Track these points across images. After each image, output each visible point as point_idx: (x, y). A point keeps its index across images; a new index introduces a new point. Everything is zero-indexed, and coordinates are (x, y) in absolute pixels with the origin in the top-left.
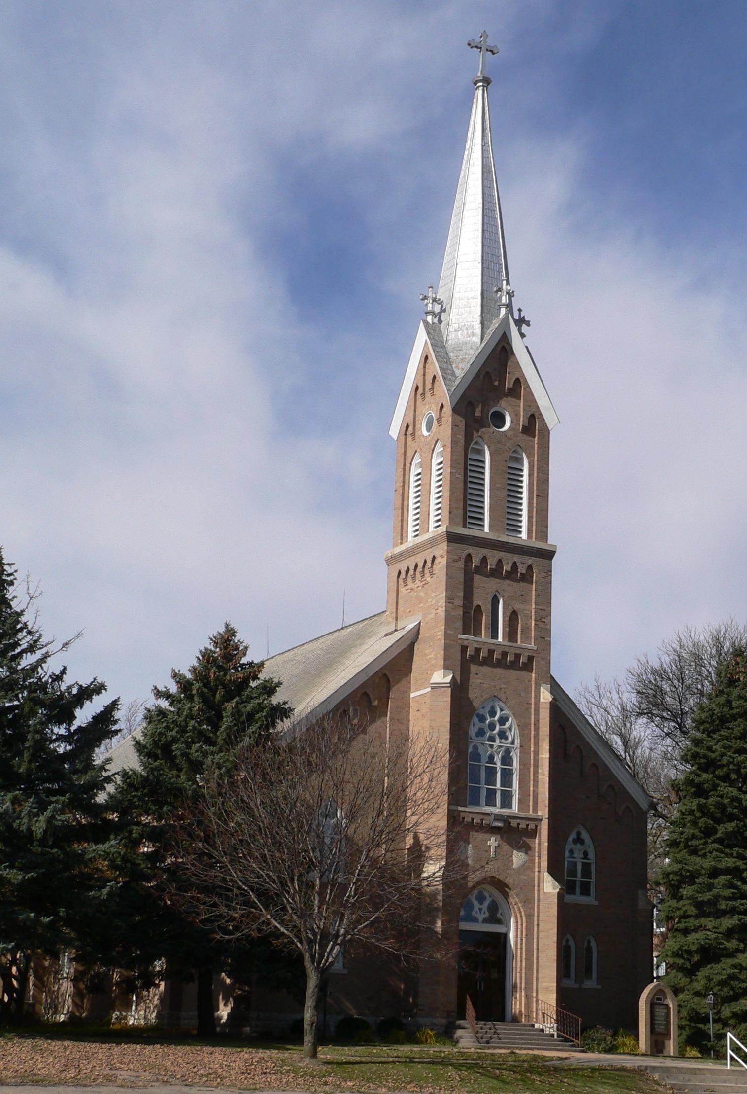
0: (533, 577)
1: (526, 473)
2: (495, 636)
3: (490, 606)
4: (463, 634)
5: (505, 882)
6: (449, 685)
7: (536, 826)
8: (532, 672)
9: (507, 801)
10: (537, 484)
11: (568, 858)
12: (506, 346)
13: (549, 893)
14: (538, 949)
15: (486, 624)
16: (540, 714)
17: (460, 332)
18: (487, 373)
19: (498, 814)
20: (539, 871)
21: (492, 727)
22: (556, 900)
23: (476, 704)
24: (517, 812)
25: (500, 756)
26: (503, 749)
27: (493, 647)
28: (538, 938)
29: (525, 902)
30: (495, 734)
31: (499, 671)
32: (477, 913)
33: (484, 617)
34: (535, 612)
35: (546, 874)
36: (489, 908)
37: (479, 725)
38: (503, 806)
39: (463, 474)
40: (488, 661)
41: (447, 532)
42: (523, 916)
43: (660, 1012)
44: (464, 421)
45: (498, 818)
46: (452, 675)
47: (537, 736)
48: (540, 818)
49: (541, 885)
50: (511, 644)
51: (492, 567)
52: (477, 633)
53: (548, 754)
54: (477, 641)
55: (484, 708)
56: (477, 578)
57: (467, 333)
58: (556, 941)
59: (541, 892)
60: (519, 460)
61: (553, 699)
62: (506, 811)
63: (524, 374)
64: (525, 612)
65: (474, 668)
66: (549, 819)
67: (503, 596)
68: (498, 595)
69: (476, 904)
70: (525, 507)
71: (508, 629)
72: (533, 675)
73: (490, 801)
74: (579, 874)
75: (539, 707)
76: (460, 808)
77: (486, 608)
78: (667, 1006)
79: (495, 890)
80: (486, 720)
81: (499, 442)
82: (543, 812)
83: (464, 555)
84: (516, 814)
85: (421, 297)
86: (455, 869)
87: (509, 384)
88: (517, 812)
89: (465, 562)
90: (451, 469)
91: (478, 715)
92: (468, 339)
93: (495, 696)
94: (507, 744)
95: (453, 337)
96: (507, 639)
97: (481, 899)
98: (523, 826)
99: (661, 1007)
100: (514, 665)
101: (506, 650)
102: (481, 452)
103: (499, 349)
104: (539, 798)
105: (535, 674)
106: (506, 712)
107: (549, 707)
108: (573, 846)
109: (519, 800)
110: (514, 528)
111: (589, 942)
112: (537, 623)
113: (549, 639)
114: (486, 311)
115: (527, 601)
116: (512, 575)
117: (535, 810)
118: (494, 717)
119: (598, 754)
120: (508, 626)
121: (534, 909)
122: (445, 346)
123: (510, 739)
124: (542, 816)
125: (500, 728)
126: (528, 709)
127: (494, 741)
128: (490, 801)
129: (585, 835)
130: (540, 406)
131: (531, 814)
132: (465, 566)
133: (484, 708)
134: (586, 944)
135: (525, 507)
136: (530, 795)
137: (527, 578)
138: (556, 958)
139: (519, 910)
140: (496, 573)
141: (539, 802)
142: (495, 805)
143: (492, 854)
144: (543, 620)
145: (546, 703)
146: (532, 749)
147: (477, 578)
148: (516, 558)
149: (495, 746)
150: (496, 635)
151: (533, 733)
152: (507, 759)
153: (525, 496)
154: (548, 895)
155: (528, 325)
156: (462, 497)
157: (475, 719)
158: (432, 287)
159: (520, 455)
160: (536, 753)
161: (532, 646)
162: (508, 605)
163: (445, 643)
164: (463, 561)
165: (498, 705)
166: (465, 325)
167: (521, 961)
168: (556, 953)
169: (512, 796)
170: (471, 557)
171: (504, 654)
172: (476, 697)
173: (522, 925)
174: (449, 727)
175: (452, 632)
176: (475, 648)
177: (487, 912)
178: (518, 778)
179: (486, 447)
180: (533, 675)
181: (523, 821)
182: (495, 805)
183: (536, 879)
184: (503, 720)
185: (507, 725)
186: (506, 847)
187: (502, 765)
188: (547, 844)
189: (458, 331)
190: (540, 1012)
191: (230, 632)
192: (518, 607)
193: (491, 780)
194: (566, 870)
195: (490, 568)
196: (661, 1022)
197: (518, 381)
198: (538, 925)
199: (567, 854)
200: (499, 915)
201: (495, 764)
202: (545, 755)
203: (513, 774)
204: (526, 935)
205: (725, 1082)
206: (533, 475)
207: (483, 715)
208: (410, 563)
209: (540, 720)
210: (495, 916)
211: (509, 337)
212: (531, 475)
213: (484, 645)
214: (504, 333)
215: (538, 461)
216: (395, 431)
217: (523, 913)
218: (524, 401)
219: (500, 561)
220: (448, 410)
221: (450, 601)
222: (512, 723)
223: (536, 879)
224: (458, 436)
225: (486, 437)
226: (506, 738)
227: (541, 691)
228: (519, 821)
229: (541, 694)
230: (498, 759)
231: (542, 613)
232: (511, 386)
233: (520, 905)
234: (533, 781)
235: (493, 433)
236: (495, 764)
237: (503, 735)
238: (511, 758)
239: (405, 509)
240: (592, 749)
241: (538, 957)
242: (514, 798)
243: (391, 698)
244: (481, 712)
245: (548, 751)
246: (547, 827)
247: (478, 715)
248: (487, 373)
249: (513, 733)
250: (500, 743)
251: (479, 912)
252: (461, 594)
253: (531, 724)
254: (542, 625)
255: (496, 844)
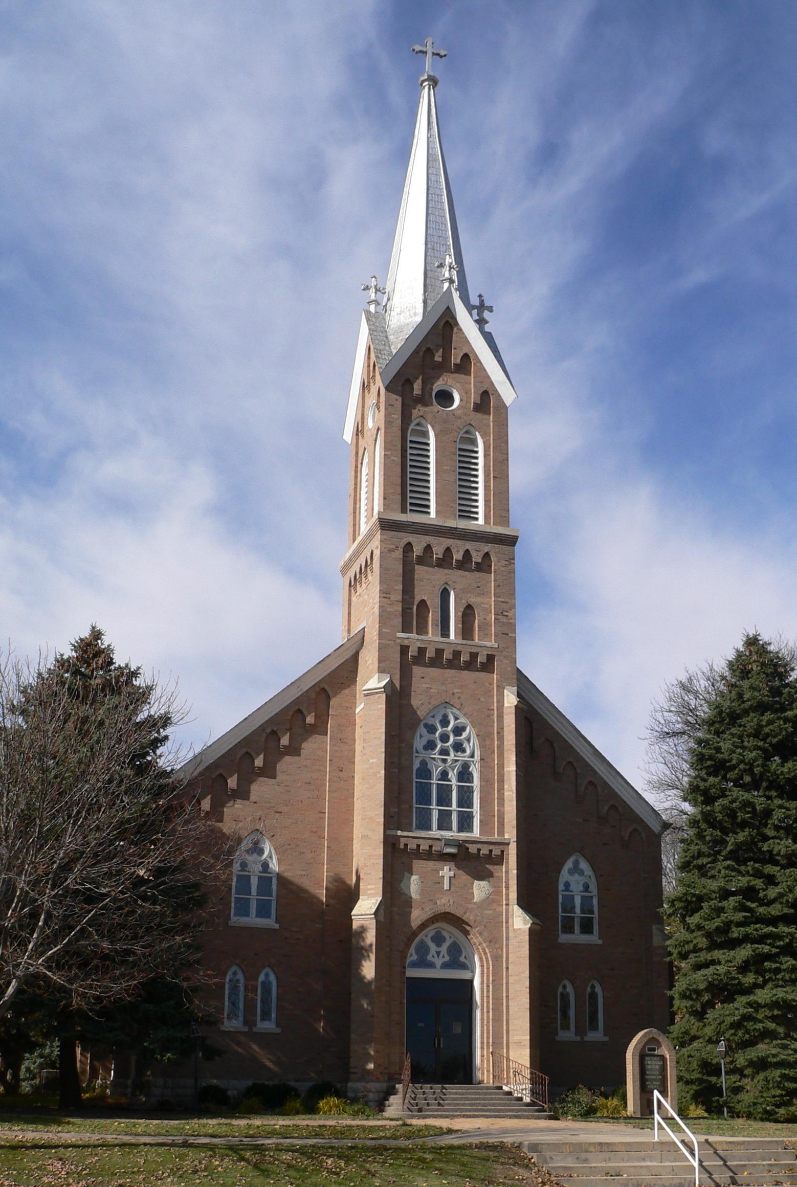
0: (491, 566)
1: (481, 455)
2: (445, 632)
3: (438, 601)
4: (403, 632)
5: (464, 918)
6: (383, 690)
7: (502, 852)
8: (493, 673)
9: (465, 822)
10: (493, 464)
11: (562, 891)
12: (451, 321)
13: (520, 929)
14: (507, 997)
15: (432, 620)
16: (505, 721)
17: (402, 315)
18: (428, 349)
19: (451, 838)
20: (507, 905)
21: (444, 738)
22: (527, 938)
23: (421, 713)
24: (478, 836)
25: (455, 771)
26: (459, 764)
27: (441, 646)
28: (507, 983)
29: (490, 941)
30: (448, 747)
31: (450, 673)
32: (433, 956)
33: (430, 613)
34: (495, 605)
35: (516, 907)
36: (449, 951)
37: (427, 737)
38: (461, 829)
39: (400, 456)
40: (437, 661)
41: (379, 518)
42: (489, 958)
43: (653, 1065)
44: (400, 399)
45: (449, 843)
46: (389, 679)
47: (501, 747)
48: (506, 842)
49: (510, 920)
50: (464, 642)
51: (438, 556)
52: (422, 630)
53: (515, 766)
54: (421, 640)
55: (433, 717)
56: (420, 570)
57: (410, 315)
58: (528, 986)
59: (510, 929)
60: (474, 442)
61: (519, 702)
62: (463, 835)
63: (473, 349)
64: (482, 605)
65: (417, 671)
66: (517, 842)
67: (454, 589)
68: (447, 587)
69: (433, 947)
70: (481, 492)
71: (461, 626)
72: (495, 677)
73: (444, 824)
74: (578, 910)
75: (503, 712)
76: (399, 833)
77: (434, 604)
78: (663, 1058)
79: (454, 928)
80: (436, 730)
81: (445, 422)
82: (511, 834)
83: (402, 544)
84: (478, 838)
85: (362, 287)
86: (173, 853)
87: (456, 359)
88: (478, 836)
89: (404, 552)
90: (385, 451)
91: (426, 726)
92: (410, 320)
93: (446, 702)
94: (464, 757)
95: (396, 321)
96: (461, 637)
97: (438, 939)
98: (485, 851)
99: (655, 1058)
100: (471, 665)
101: (459, 648)
102: (425, 434)
103: (442, 323)
104: (505, 819)
105: (497, 675)
106: (462, 720)
107: (514, 711)
108: (570, 877)
109: (481, 821)
110: (467, 513)
111: (593, 987)
112: (498, 617)
113: (513, 635)
114: (430, 290)
115: (486, 594)
116: (465, 563)
117: (501, 832)
118: (447, 727)
119: (596, 771)
120: (461, 622)
121: (502, 949)
122: (386, 332)
123: (468, 752)
124: (510, 839)
125: (454, 740)
126: (490, 716)
127: (448, 755)
128: (444, 824)
129: (584, 865)
130: (493, 381)
131: (496, 837)
132: (404, 556)
133: (433, 717)
134: (589, 990)
135: (481, 492)
136: (494, 816)
137: (484, 566)
138: (528, 1006)
139: (484, 951)
140: (445, 561)
141: (505, 824)
142: (450, 829)
143: (446, 887)
144: (506, 614)
145: (510, 707)
146: (496, 762)
147: (420, 570)
148: (469, 545)
149: (449, 760)
150: (447, 633)
151: (496, 743)
152: (465, 775)
153: (481, 479)
154: (518, 932)
155: (491, 311)
156: (399, 481)
157: (422, 730)
158: (375, 277)
159: (473, 435)
160: (501, 766)
161: (492, 643)
162: (461, 599)
163: (379, 643)
164: (402, 550)
165: (452, 712)
166: (407, 307)
167: (488, 1012)
168: (528, 1000)
169: (473, 817)
170: (412, 546)
171: (457, 654)
172: (422, 704)
173: (488, 968)
174: (384, 738)
175: (389, 631)
176: (419, 648)
177: (446, 955)
178: (479, 796)
179: (430, 427)
180: (495, 677)
181: (485, 845)
182: (450, 829)
183: (504, 914)
184: (458, 731)
185: (464, 735)
186: (464, 877)
187: (459, 781)
188: (515, 872)
189: (400, 314)
190: (511, 1071)
191: (97, 635)
192: (473, 600)
193: (444, 799)
194: (560, 905)
195: (436, 558)
196: (654, 1077)
197: (466, 357)
198: (507, 968)
199: (561, 887)
200: (462, 959)
201: (450, 781)
202: (511, 768)
203: (473, 792)
204: (493, 981)
205: (644, 1160)
206: (490, 455)
207: (432, 725)
208: (356, 568)
209: (505, 728)
210: (457, 959)
211: (453, 311)
212: (486, 456)
213: (429, 644)
214: (448, 308)
215: (493, 439)
216: (348, 435)
217: (489, 955)
218: (474, 378)
219: (448, 550)
220: (383, 391)
221: (385, 595)
222: (470, 733)
223: (504, 914)
224: (393, 416)
225: (429, 417)
226: (464, 751)
227: (505, 694)
228: (479, 846)
229: (505, 698)
230: (453, 776)
231: (504, 605)
232: (458, 361)
233: (484, 945)
234: (498, 799)
235: (438, 412)
236: (450, 781)
237: (458, 747)
238: (471, 774)
239: (357, 512)
240: (587, 765)
241: (508, 1006)
242: (475, 819)
243: (332, 715)
244: (430, 721)
245: (515, 762)
246: (515, 852)
247: (426, 726)
248: (428, 349)
249: (471, 744)
250: (455, 756)
251: (436, 955)
252: (400, 587)
253: (494, 734)
254: (504, 620)
255: (452, 874)
